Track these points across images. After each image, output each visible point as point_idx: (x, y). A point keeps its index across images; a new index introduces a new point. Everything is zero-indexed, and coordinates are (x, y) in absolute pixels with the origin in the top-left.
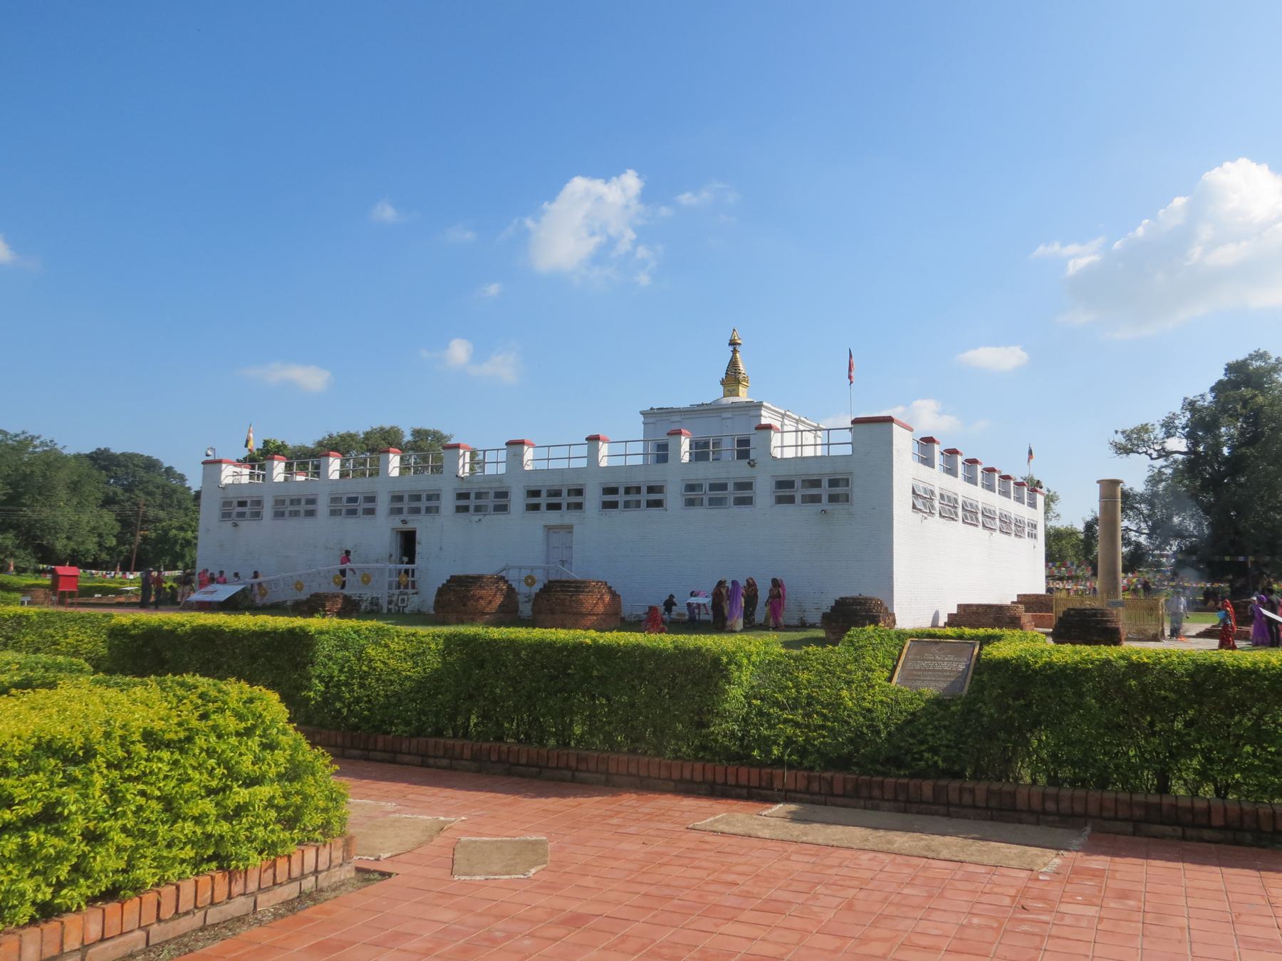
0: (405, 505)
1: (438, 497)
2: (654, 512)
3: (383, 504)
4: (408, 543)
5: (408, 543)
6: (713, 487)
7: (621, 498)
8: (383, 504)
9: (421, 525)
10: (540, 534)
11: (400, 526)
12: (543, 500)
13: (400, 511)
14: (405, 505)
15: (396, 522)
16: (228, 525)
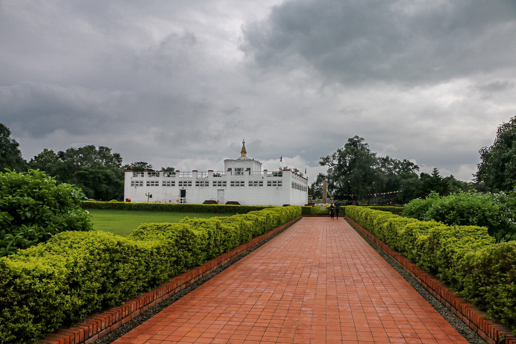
0: (183, 184)
1: (191, 182)
2: (207, 187)
3: (177, 184)
4: (183, 193)
5: (183, 193)
6: (219, 182)
7: (200, 184)
8: (177, 184)
9: (186, 188)
10: (216, 191)
11: (182, 189)
12: (217, 184)
13: (181, 185)
14: (183, 184)
15: (181, 188)
16: (133, 187)
